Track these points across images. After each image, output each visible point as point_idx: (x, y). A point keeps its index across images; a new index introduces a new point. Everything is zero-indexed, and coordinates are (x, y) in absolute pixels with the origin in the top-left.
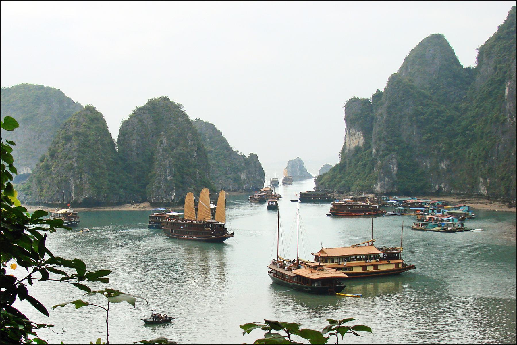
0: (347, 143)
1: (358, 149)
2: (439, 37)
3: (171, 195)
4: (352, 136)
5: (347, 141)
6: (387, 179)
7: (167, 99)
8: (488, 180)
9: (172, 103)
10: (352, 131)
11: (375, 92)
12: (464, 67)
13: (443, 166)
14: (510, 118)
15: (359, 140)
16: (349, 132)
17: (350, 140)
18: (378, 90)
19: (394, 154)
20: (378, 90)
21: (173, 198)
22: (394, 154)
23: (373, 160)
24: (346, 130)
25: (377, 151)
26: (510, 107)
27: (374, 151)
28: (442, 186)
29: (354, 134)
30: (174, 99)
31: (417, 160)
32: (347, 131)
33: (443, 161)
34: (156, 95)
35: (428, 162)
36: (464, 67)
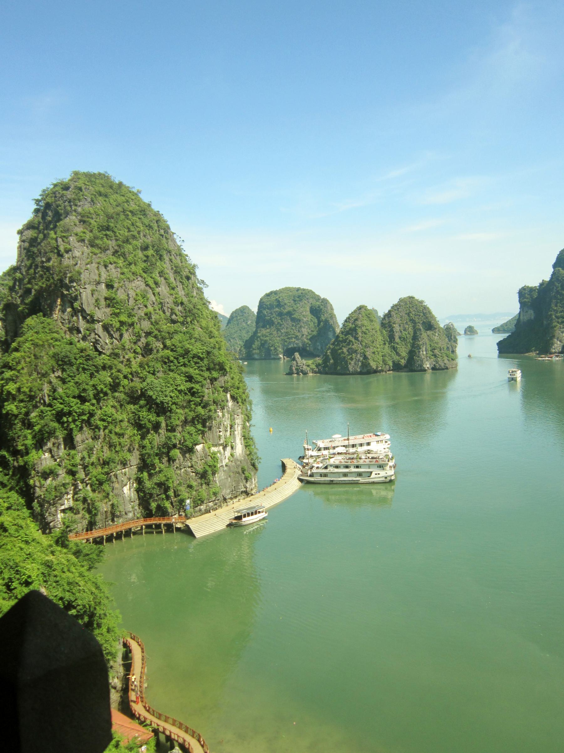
0: (521, 318)
3: (426, 364)
6: (559, 343)
7: (413, 298)
9: (417, 300)
11: (541, 281)
15: (531, 314)
16: (523, 310)
17: (523, 316)
18: (543, 280)
20: (543, 280)
21: (428, 366)
24: (520, 309)
27: (545, 322)
29: (527, 312)
30: (418, 296)
34: (404, 295)
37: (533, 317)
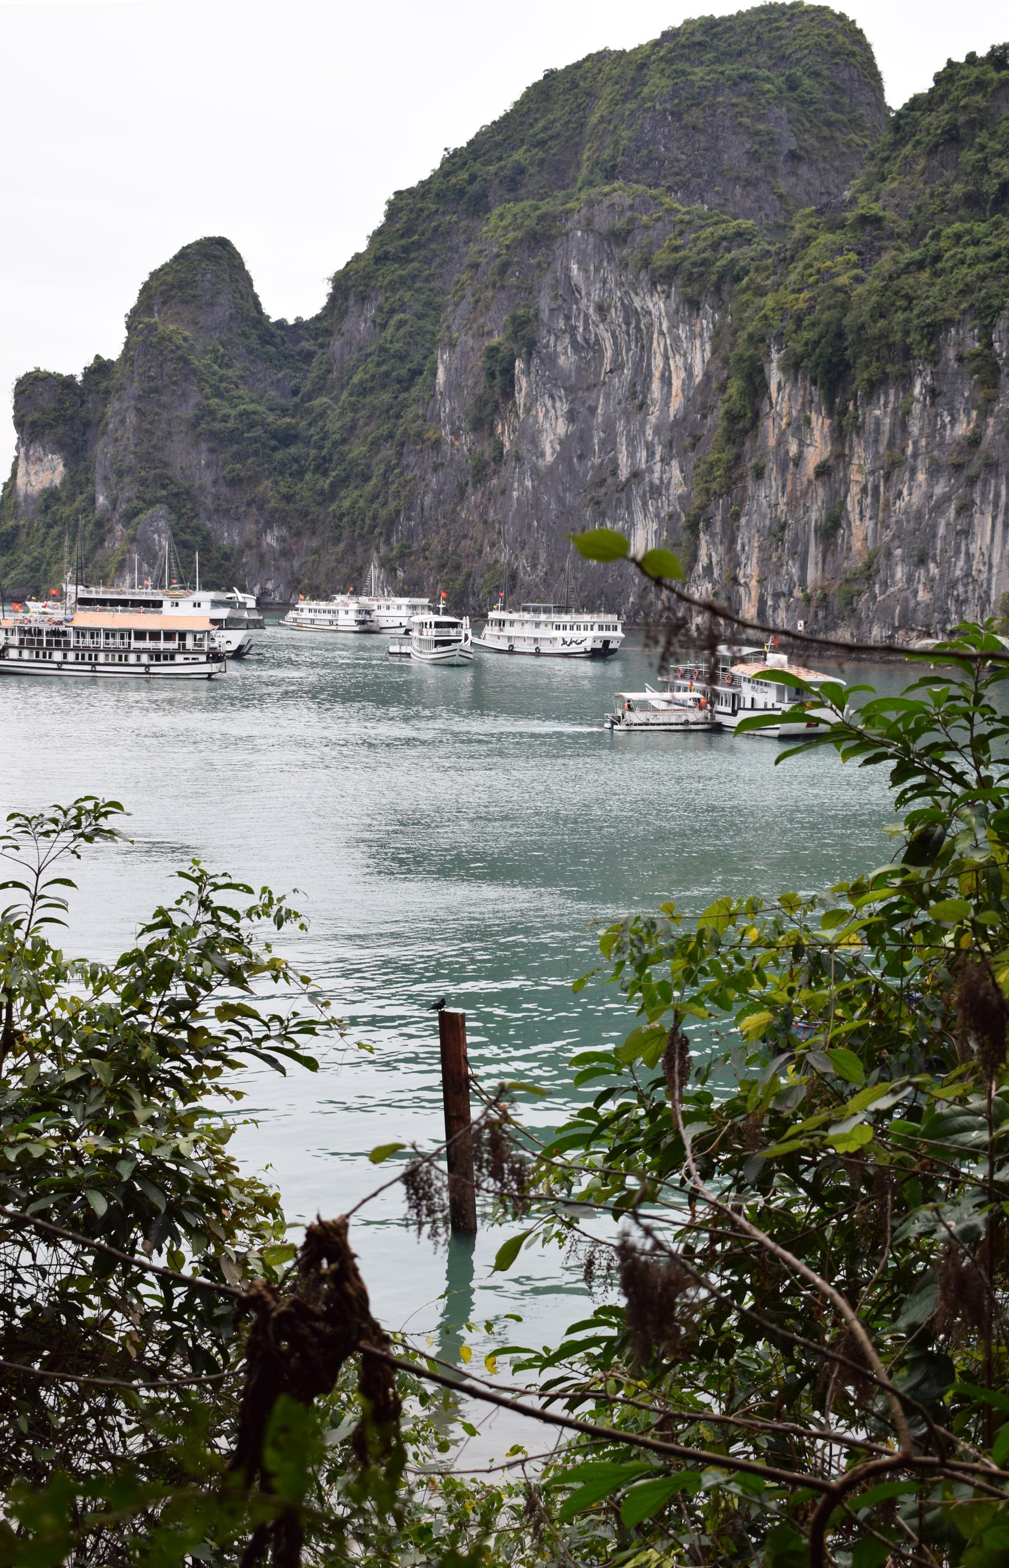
0: (21, 481)
1: (51, 496)
2: (223, 243)
4: (34, 463)
5: (20, 474)
8: (400, 574)
10: (36, 450)
12: (272, 320)
13: (270, 540)
14: (452, 434)
16: (27, 451)
17: (28, 474)
18: (98, 357)
19: (161, 509)
20: (98, 357)
22: (161, 509)
23: (99, 524)
24: (17, 448)
25: (114, 502)
26: (453, 410)
27: (101, 499)
28: (270, 586)
29: (41, 460)
31: (209, 525)
32: (22, 450)
33: (271, 528)
35: (236, 532)
36: (272, 320)
37: (57, 482)
